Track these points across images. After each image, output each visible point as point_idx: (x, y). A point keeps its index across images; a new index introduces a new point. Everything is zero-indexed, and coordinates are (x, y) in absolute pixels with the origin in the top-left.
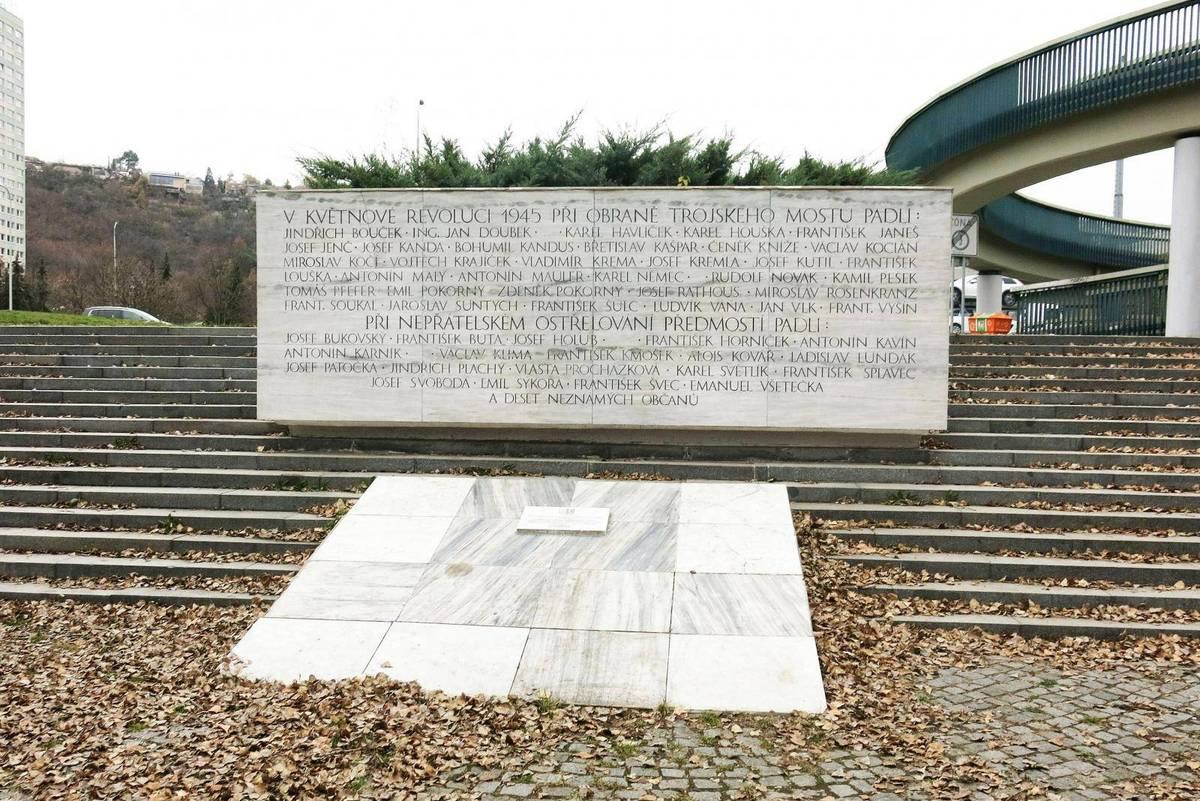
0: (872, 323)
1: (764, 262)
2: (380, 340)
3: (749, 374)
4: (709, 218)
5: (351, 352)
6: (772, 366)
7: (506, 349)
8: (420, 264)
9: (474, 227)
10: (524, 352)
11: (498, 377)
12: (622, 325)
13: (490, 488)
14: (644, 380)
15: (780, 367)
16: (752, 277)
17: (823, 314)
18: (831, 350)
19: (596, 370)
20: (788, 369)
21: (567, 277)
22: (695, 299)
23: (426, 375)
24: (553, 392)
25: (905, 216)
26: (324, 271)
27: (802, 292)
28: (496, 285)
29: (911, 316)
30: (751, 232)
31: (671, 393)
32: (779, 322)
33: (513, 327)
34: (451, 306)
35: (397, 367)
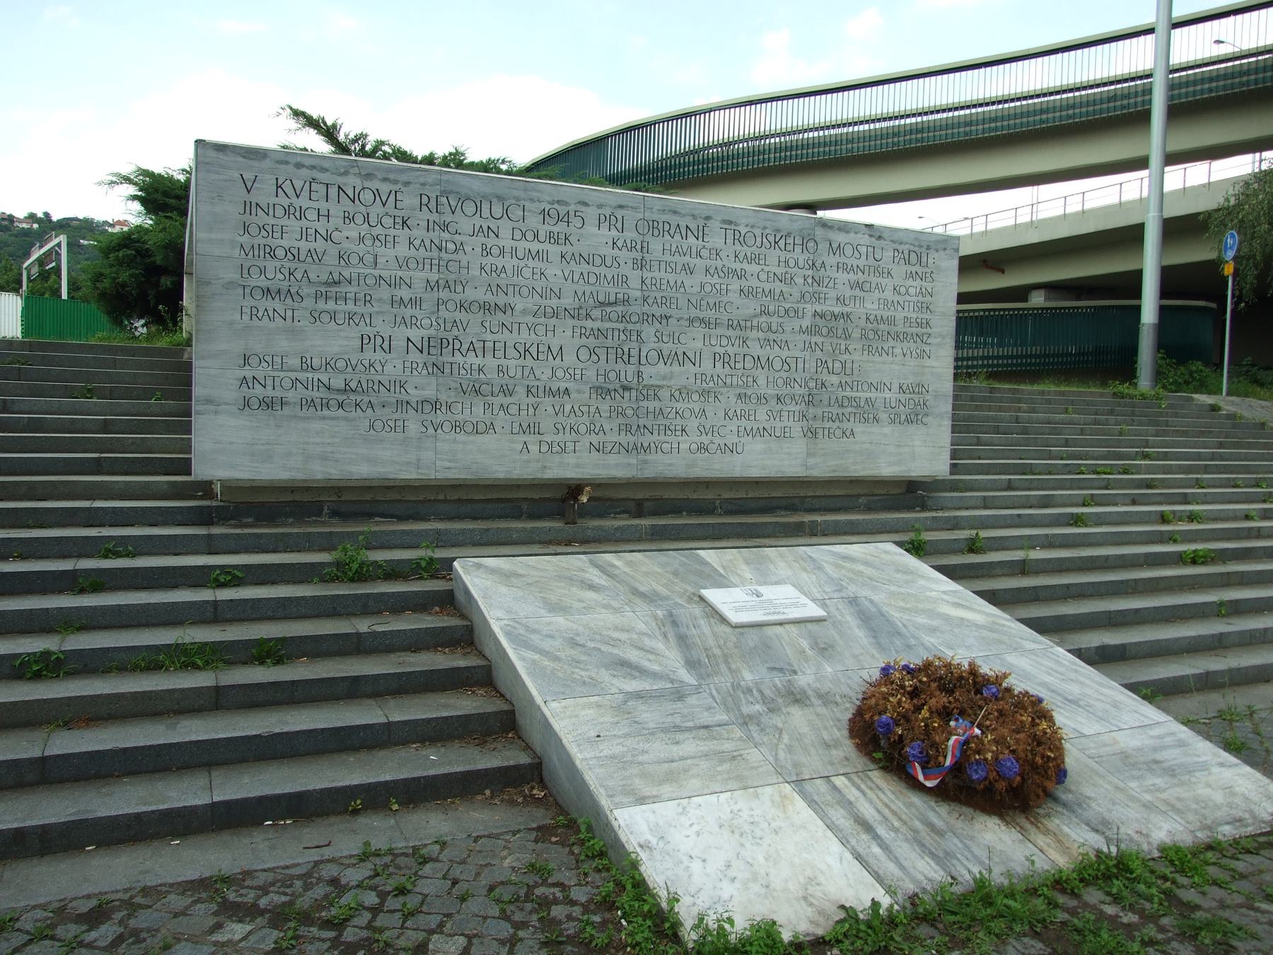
2: (379, 368)
4: (759, 243)
5: (338, 382)
8: (435, 268)
9: (505, 227)
14: (693, 424)
15: (819, 412)
17: (856, 357)
19: (642, 412)
21: (612, 299)
22: (742, 333)
23: (440, 417)
24: (594, 439)
25: (924, 259)
27: (840, 331)
29: (927, 362)
30: (796, 263)
31: (717, 440)
33: (550, 357)
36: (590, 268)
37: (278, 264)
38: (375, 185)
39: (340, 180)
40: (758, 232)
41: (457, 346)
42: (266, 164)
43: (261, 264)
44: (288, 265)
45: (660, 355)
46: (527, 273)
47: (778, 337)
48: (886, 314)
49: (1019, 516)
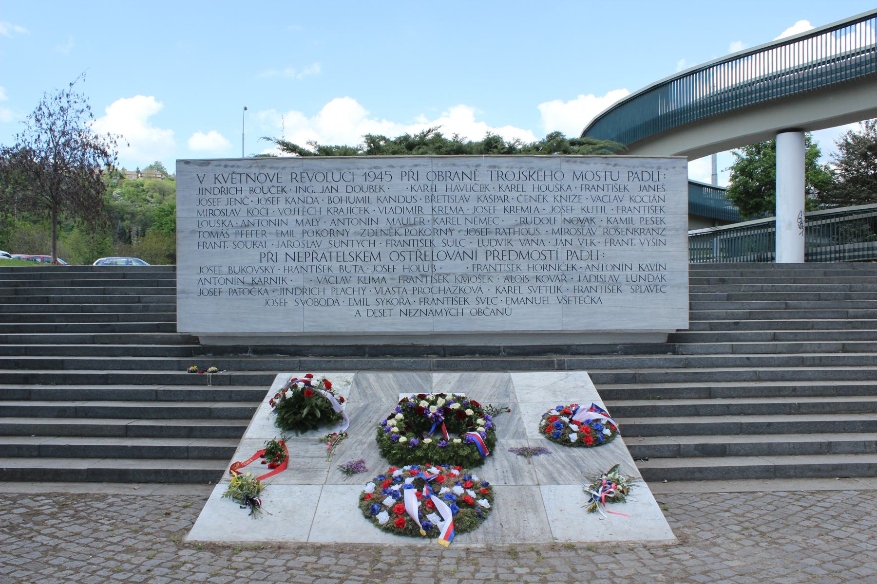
0: (635, 253)
1: (557, 210)
2: (271, 271)
3: (548, 292)
5: (248, 280)
6: (565, 285)
7: (367, 276)
8: (301, 213)
9: (342, 186)
13: (367, 380)
14: (471, 298)
15: (571, 286)
16: (549, 220)
17: (601, 247)
18: (608, 274)
19: (435, 290)
22: (508, 237)
23: (306, 297)
24: (403, 308)
25: (656, 176)
26: (228, 219)
28: (359, 228)
29: (662, 248)
30: (547, 188)
31: (491, 307)
32: (569, 253)
34: (325, 245)
35: (284, 290)
36: (397, 204)
37: (216, 218)
38: (266, 171)
39: (247, 171)
40: (516, 171)
41: (315, 255)
42: (210, 167)
43: (208, 219)
44: (221, 218)
45: (447, 254)
46: (356, 210)
47: (535, 238)
48: (624, 217)
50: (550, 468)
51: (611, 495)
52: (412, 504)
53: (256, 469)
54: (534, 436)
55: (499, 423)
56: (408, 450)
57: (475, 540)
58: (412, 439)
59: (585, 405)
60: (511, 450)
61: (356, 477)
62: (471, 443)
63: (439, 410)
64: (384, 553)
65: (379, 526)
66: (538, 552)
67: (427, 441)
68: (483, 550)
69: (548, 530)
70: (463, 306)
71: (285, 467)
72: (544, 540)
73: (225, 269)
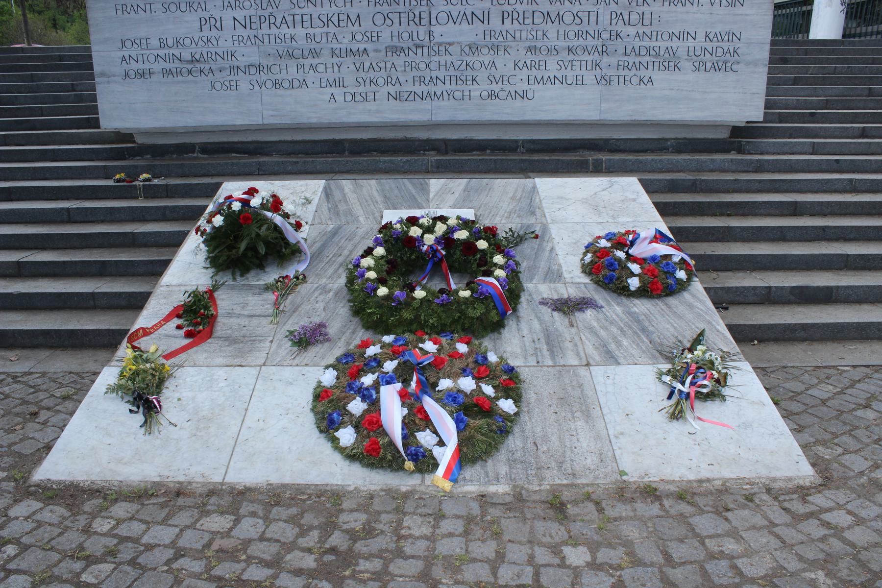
2: (215, 43)
3: (584, 68)
5: (187, 56)
6: (606, 59)
7: (343, 47)
10: (361, 50)
11: (337, 76)
12: (459, 20)
13: (342, 190)
15: (613, 61)
18: (663, 45)
19: (434, 66)
20: (621, 63)
23: (264, 76)
24: (392, 90)
31: (508, 88)
32: (614, 16)
33: (350, 24)
41: (272, 21)
45: (450, 15)
49: (837, 161)
50: (602, 333)
51: (705, 391)
52: (393, 413)
53: (171, 336)
54: (575, 281)
55: (523, 253)
56: (390, 308)
57: (493, 479)
58: (397, 292)
59: (646, 233)
60: (544, 303)
61: (314, 351)
62: (486, 298)
63: (438, 241)
64: (346, 504)
65: (341, 450)
66: (597, 504)
67: (419, 293)
68: (508, 499)
69: (610, 454)
70: (471, 87)
71: (210, 335)
72: (605, 479)
73: (155, 42)
